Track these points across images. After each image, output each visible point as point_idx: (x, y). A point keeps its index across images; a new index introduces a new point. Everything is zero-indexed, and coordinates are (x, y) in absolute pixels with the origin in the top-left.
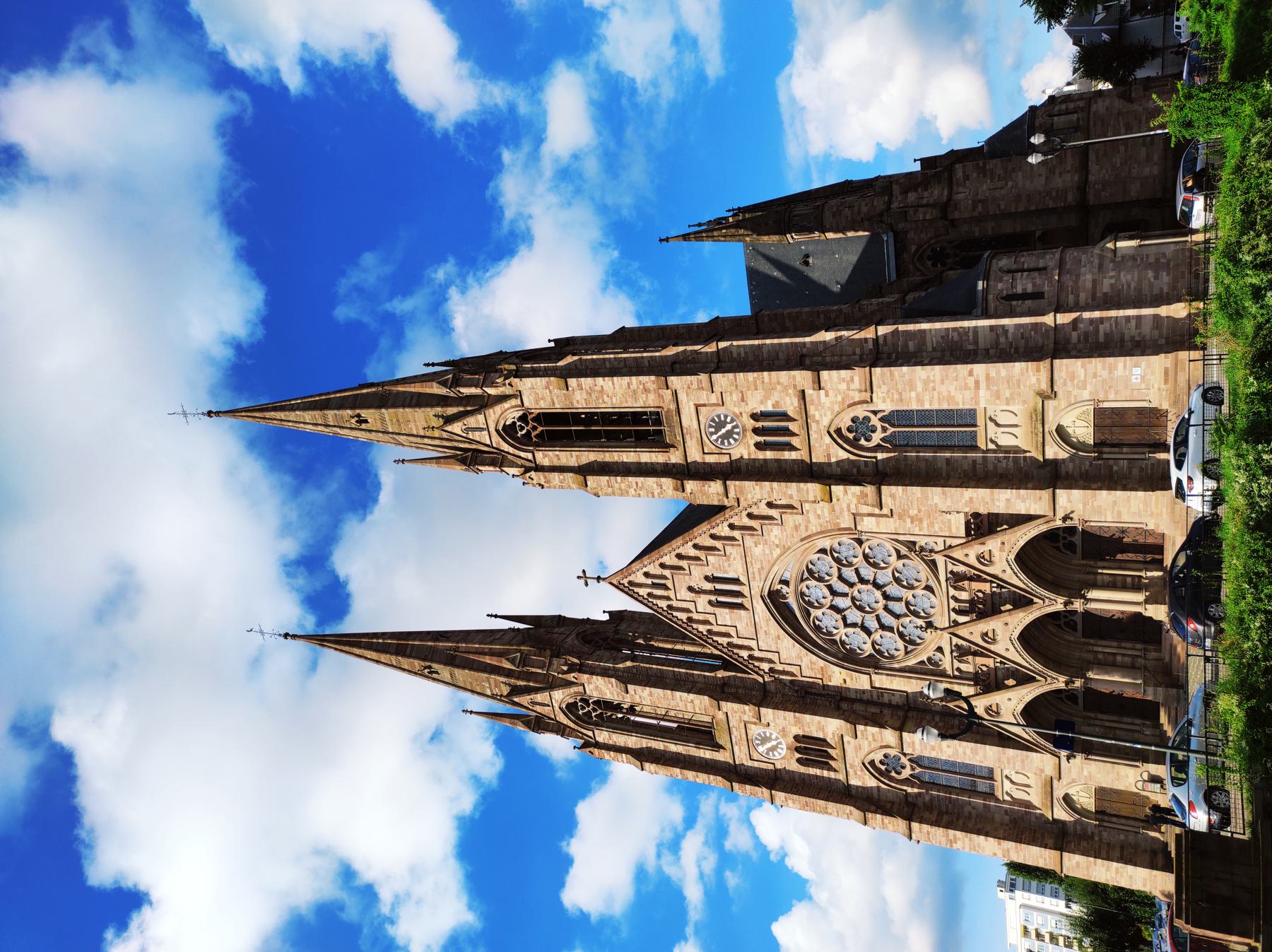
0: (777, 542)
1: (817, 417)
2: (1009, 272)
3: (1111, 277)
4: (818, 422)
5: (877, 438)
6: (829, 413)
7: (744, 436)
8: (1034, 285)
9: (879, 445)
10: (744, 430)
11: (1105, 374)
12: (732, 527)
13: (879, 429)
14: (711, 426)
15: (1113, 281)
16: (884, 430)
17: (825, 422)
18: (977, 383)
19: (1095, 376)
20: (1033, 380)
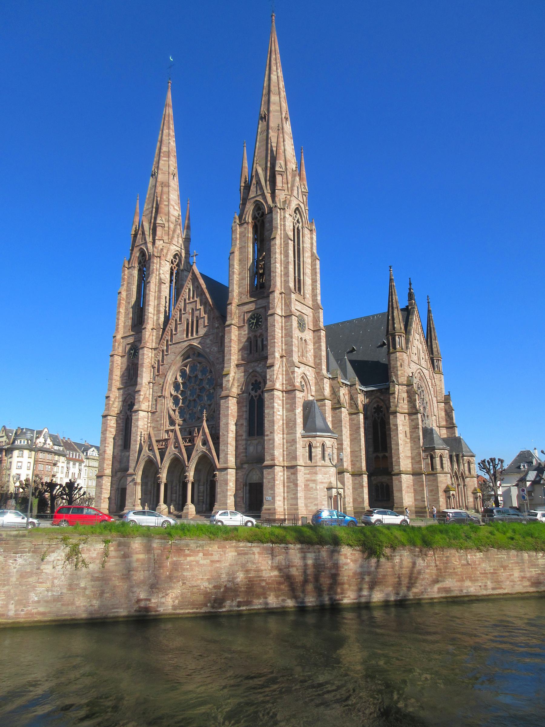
0: (212, 350)
1: (260, 365)
2: (323, 445)
3: (316, 487)
4: (258, 366)
5: (253, 393)
6: (261, 371)
7: (253, 331)
8: (315, 456)
9: (250, 394)
10: (255, 331)
11: (270, 486)
12: (218, 328)
13: (257, 394)
14: (257, 314)
15: (314, 488)
16: (256, 396)
17: (258, 369)
18: (267, 435)
19: (269, 482)
20: (268, 458)
